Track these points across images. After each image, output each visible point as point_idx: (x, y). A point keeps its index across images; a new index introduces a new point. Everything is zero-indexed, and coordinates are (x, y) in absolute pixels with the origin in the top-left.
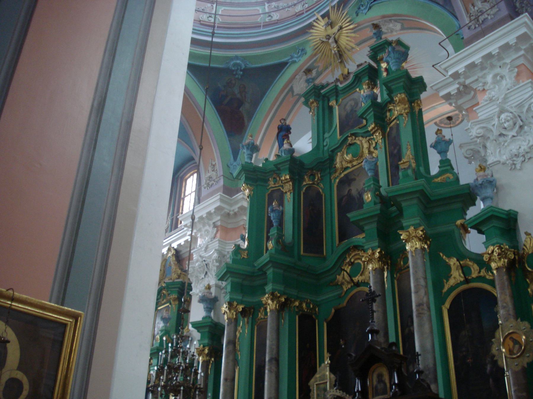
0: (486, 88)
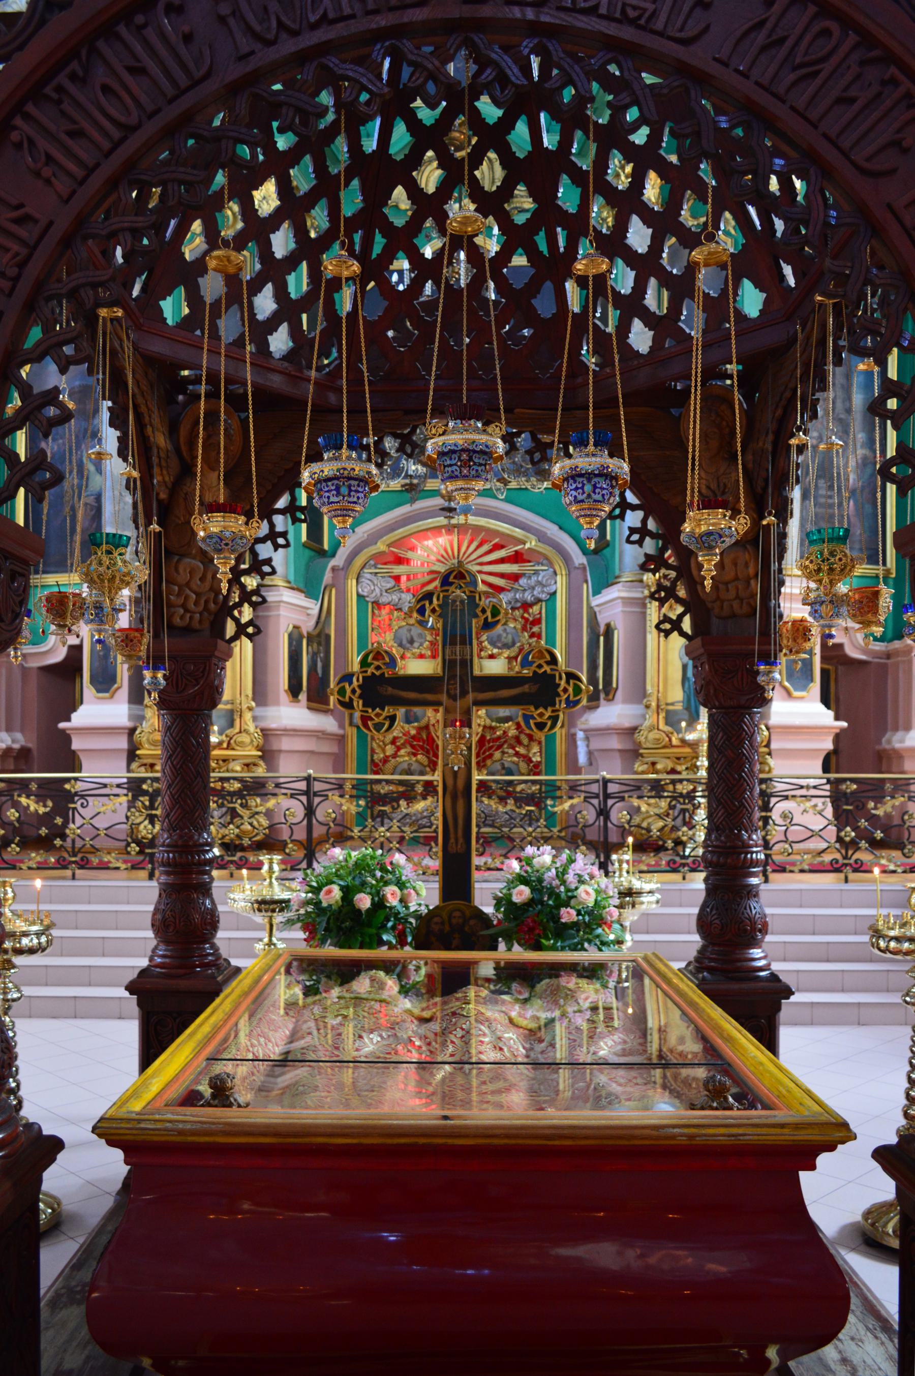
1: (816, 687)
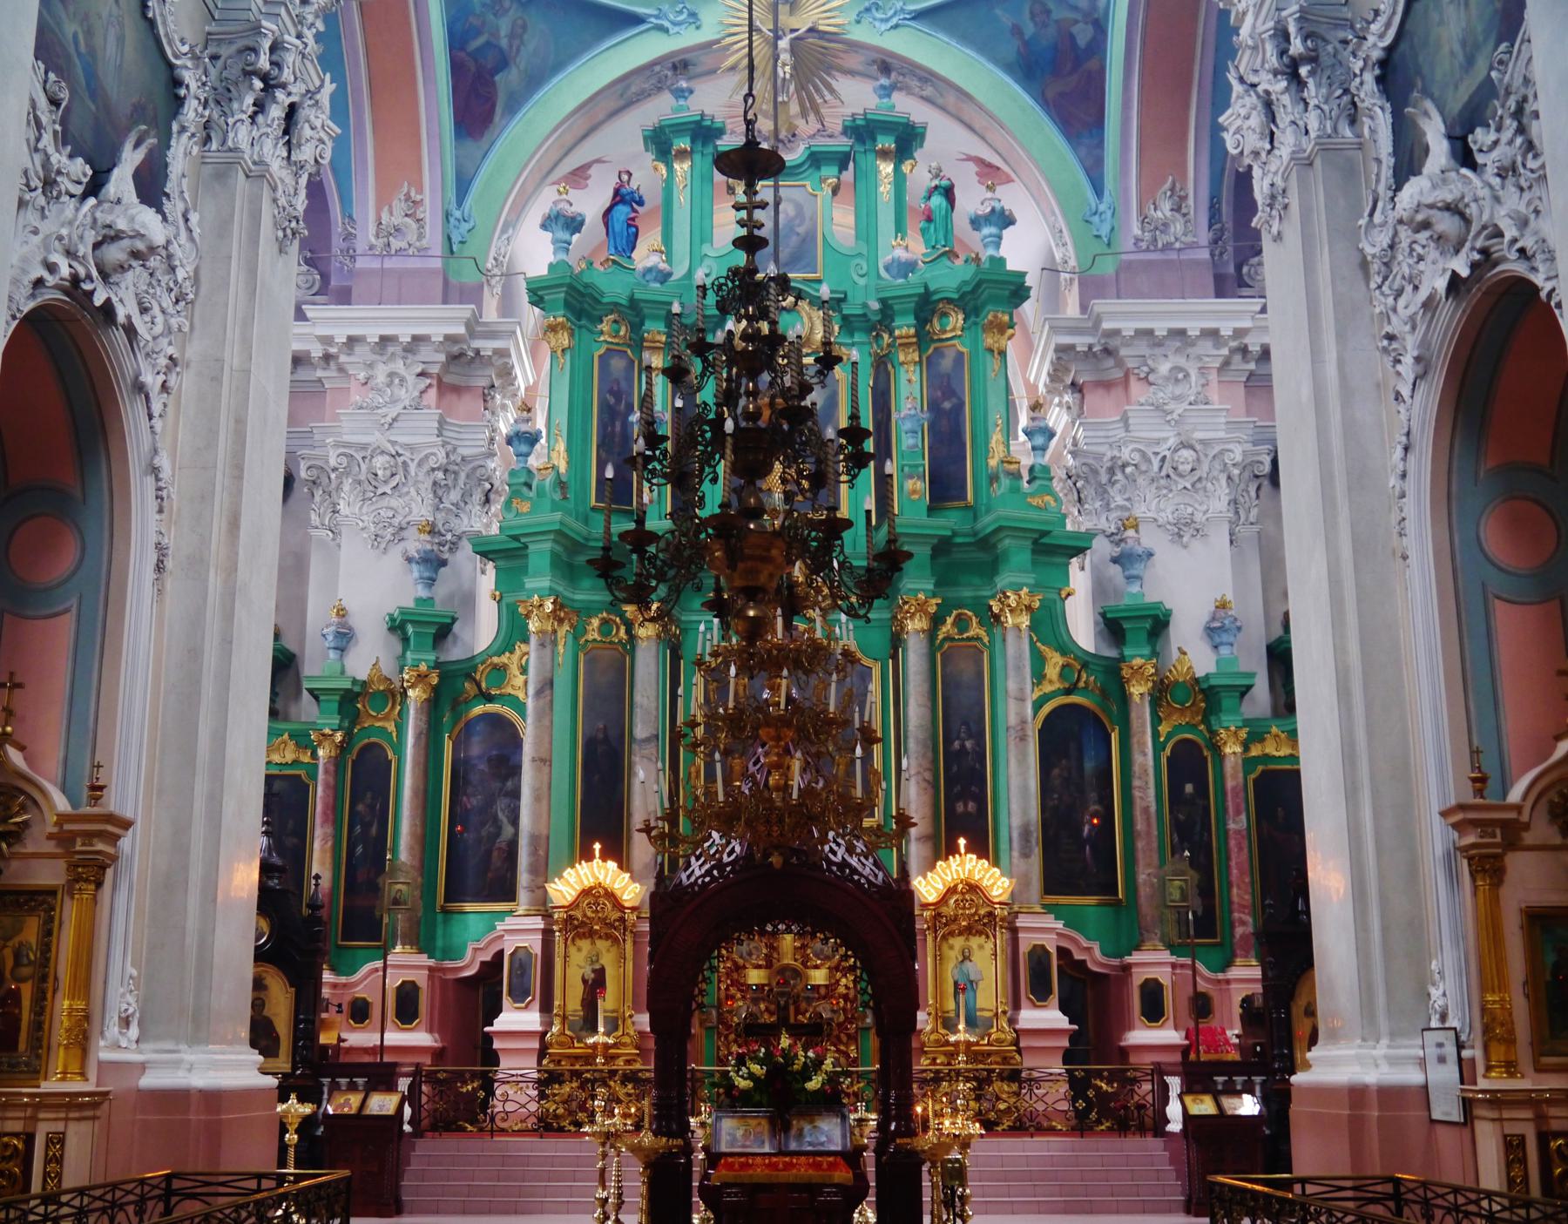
0: (1151, 378)
1: (1054, 999)
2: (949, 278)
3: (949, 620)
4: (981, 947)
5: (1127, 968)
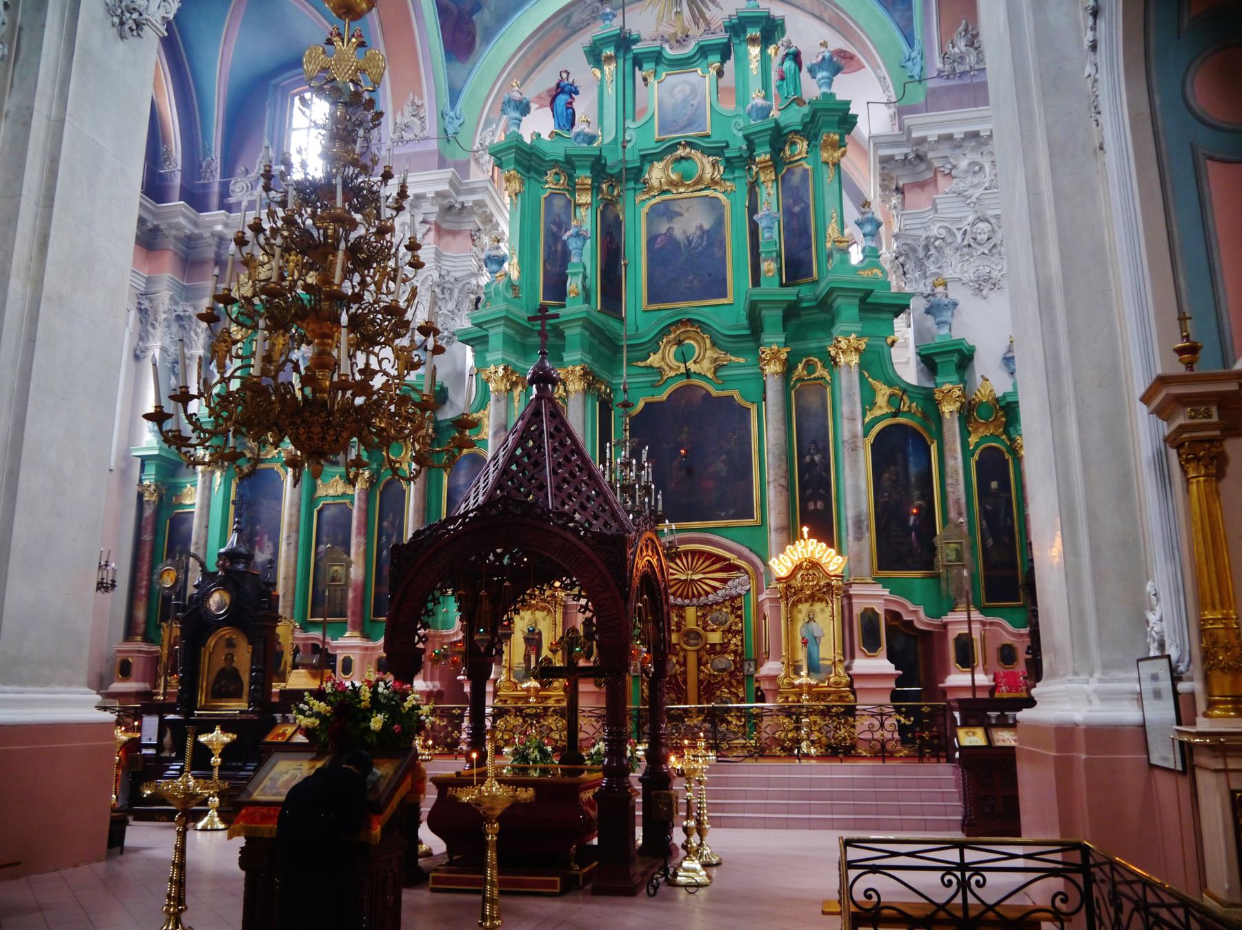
0: (954, 173)
2: (794, 117)
3: (800, 366)
4: (822, 610)
5: (945, 626)
